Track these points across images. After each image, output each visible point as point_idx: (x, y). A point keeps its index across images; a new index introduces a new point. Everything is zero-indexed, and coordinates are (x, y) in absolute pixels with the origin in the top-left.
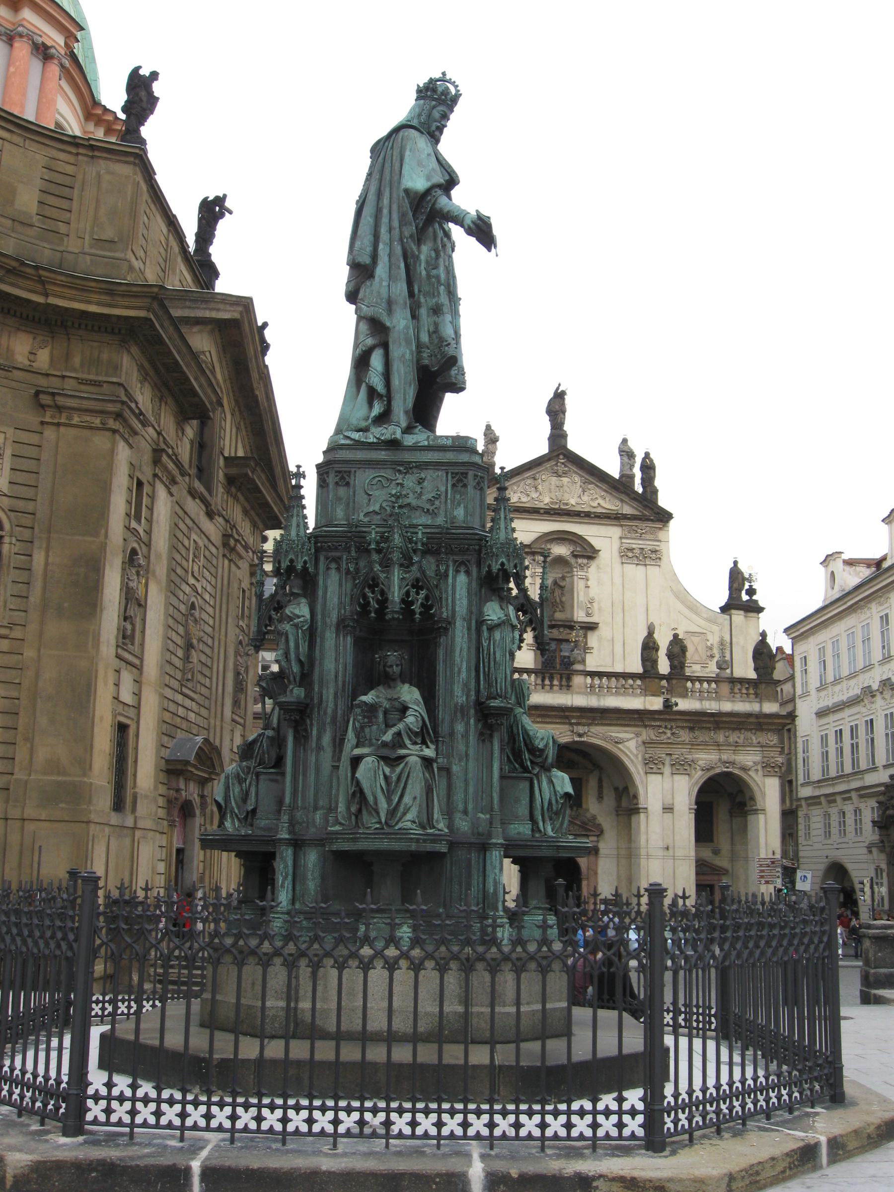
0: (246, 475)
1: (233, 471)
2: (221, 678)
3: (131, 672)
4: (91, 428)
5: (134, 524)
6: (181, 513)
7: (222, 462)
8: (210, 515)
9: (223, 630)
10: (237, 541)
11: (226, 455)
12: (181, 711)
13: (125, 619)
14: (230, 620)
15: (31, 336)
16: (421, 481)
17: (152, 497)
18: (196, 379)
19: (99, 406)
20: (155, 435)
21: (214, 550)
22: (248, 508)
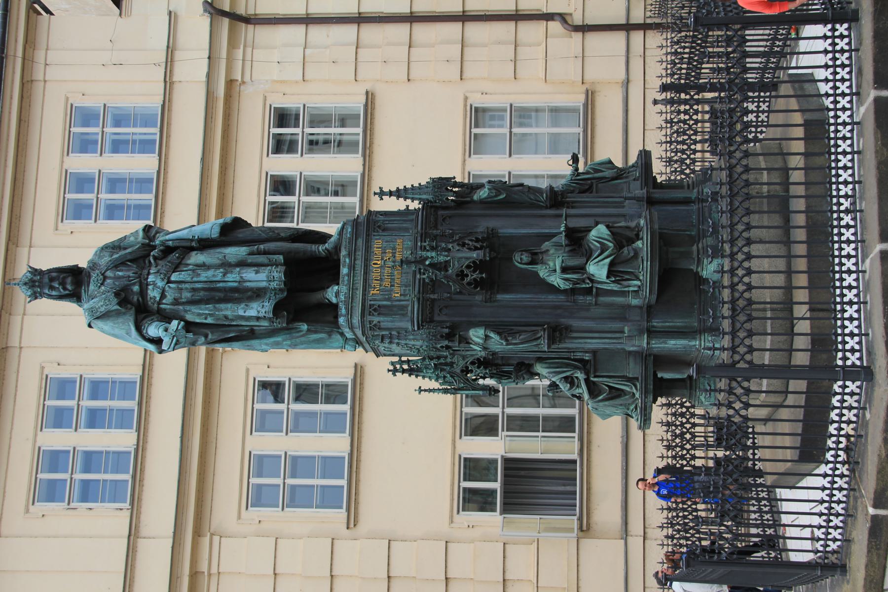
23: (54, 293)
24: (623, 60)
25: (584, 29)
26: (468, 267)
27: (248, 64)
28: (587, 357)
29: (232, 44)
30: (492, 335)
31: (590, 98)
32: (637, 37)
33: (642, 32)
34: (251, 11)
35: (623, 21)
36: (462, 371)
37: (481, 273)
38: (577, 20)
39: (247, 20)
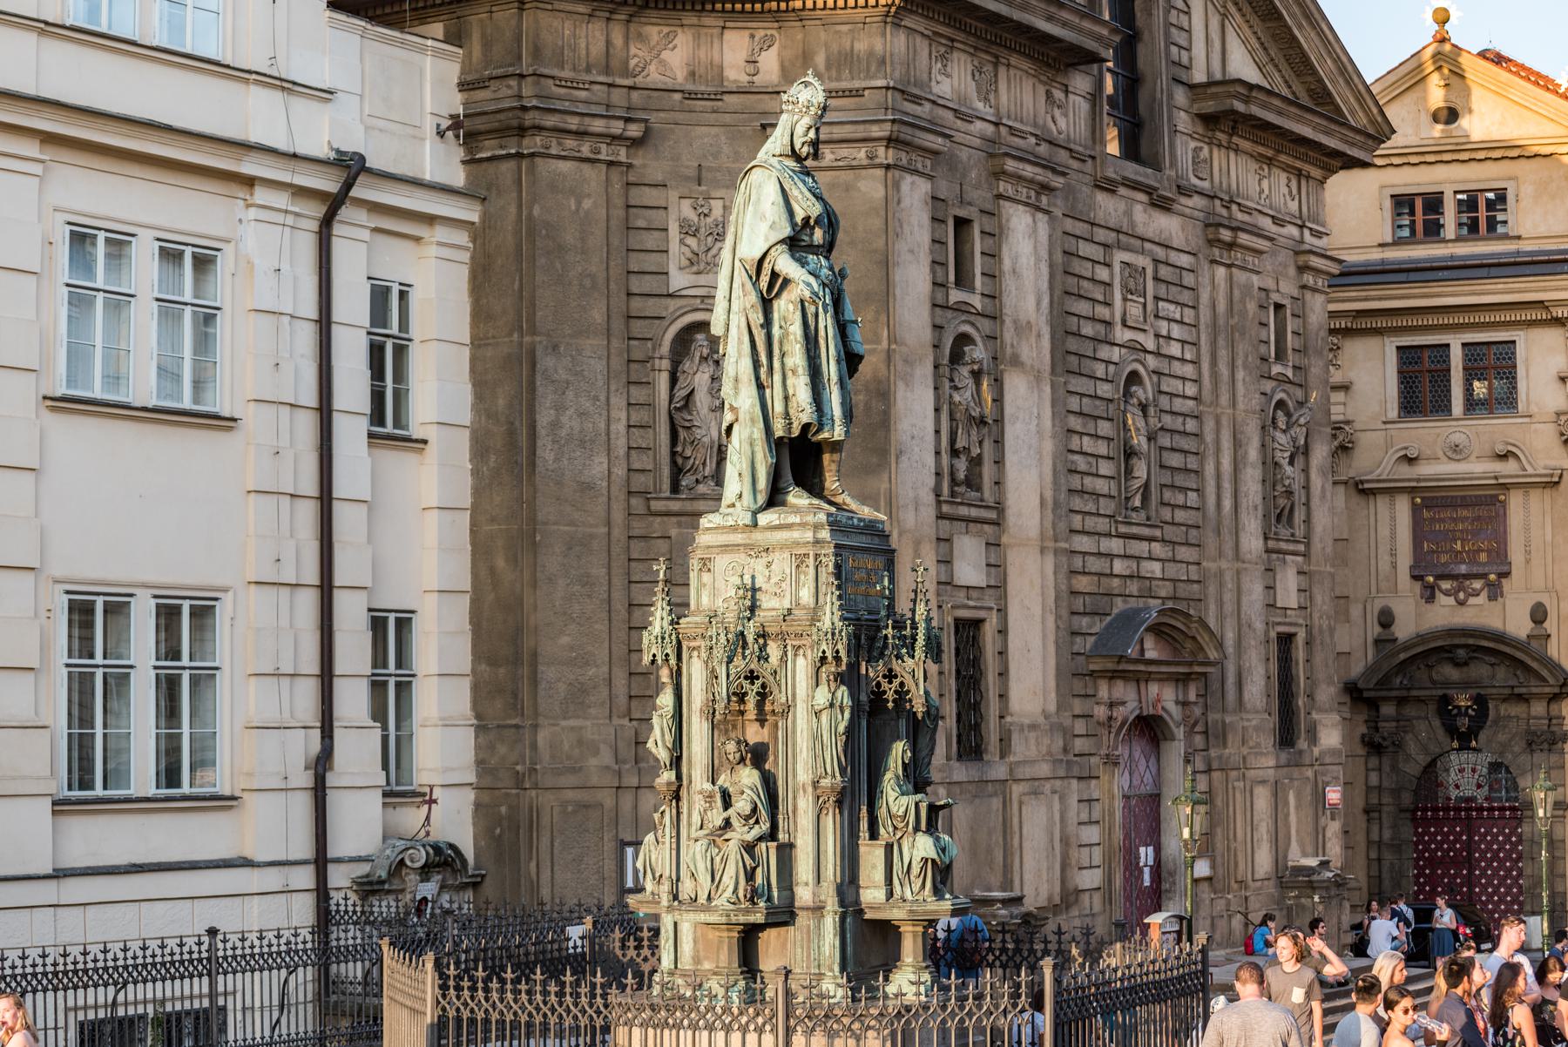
0: (1234, 112)
1: (1209, 106)
2: (1227, 485)
3: (979, 534)
4: (852, 168)
5: (956, 296)
6: (1080, 228)
7: (1180, 96)
8: (1161, 204)
9: (1224, 399)
10: (1235, 229)
11: (1199, 76)
12: (1119, 566)
13: (955, 453)
14: (1240, 374)
15: (747, 33)
16: (769, 565)
17: (995, 235)
18: (1050, 18)
19: (860, 132)
20: (990, 129)
21: (1184, 260)
22: (1270, 153)
23: (800, 130)
24: (282, 857)
25: (320, 792)
26: (902, 684)
27: (280, 218)
28: (782, 837)
29: (300, 192)
30: (847, 715)
31: (224, 802)
32: (304, 878)
33: (312, 885)
34: (337, 229)
35: (332, 853)
36: (752, 672)
37: (894, 701)
38: (331, 779)
39: (327, 223)
